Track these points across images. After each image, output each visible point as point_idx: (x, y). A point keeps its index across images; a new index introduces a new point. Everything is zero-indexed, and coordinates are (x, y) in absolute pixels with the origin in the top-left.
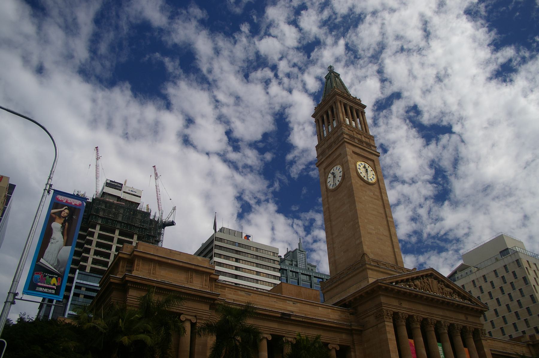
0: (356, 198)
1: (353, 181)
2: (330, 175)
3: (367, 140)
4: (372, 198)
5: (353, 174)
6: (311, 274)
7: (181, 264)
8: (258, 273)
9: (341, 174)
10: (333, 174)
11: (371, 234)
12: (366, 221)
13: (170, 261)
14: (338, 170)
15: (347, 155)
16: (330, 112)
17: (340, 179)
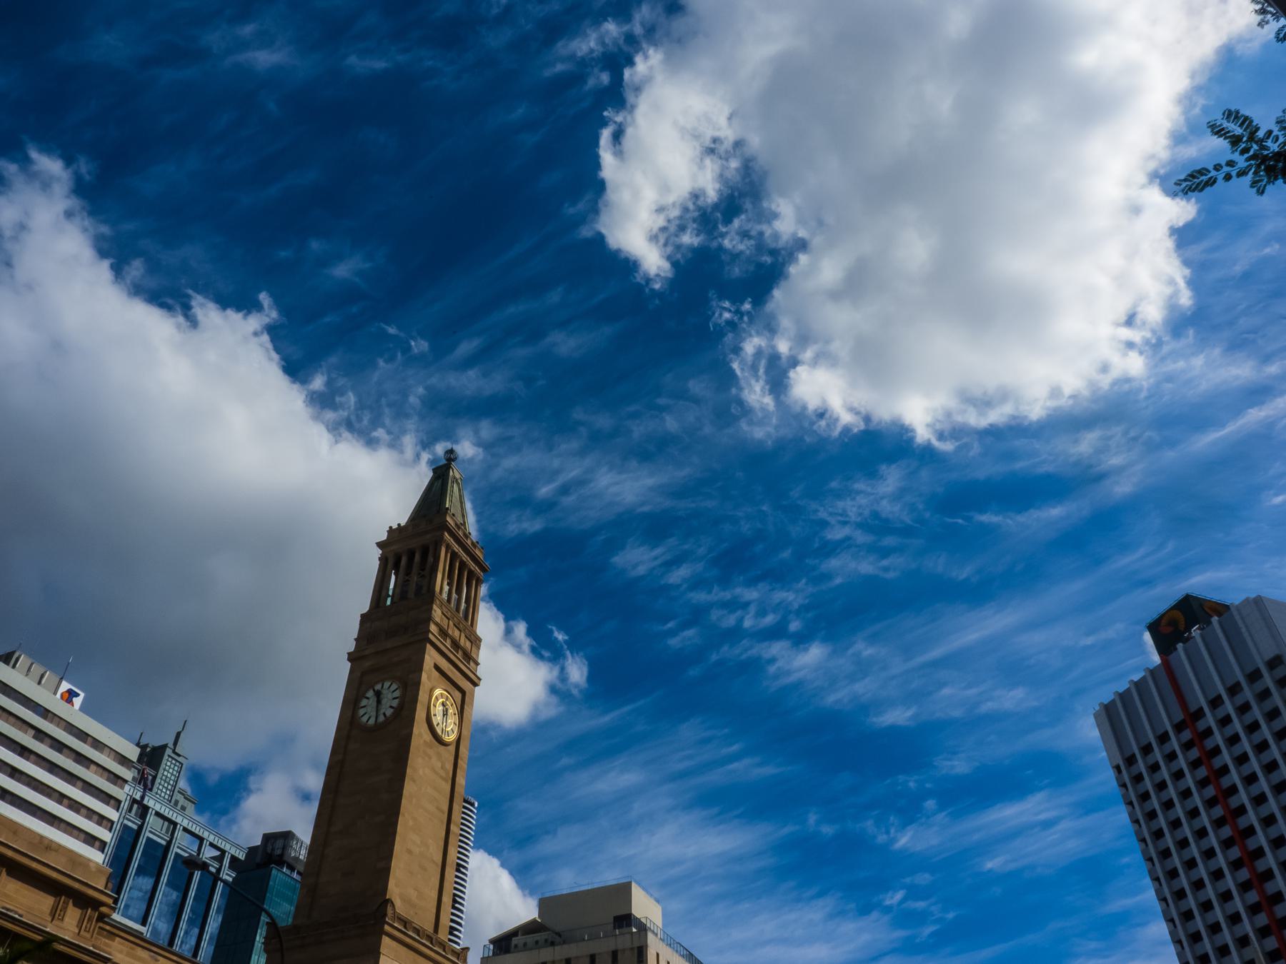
0: (408, 770)
1: (415, 731)
2: (370, 694)
3: (468, 644)
4: (436, 773)
5: (420, 715)
6: (179, 820)
7: (54, 875)
8: (61, 798)
9: (395, 703)
10: (378, 694)
11: (410, 852)
12: (411, 823)
13: (34, 865)
14: (391, 694)
15: (421, 670)
16: (417, 558)
17: (389, 712)
